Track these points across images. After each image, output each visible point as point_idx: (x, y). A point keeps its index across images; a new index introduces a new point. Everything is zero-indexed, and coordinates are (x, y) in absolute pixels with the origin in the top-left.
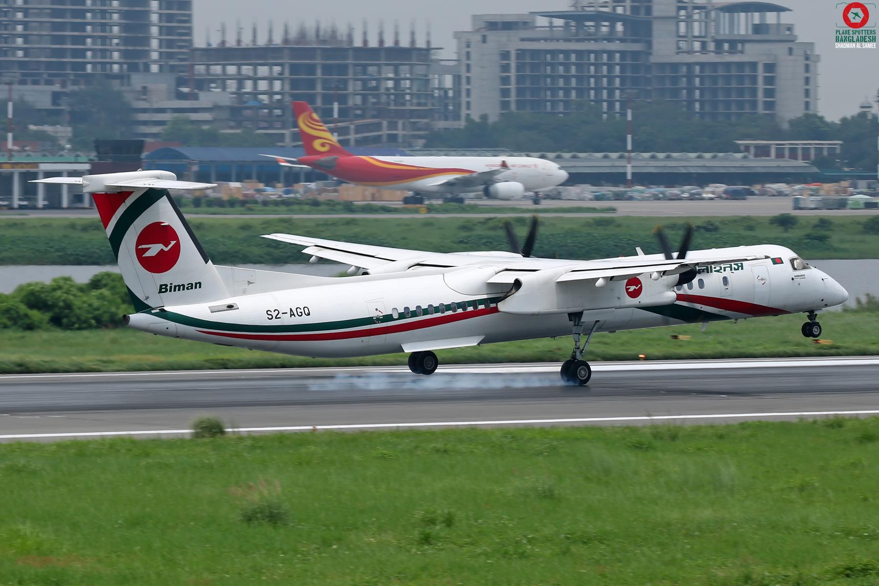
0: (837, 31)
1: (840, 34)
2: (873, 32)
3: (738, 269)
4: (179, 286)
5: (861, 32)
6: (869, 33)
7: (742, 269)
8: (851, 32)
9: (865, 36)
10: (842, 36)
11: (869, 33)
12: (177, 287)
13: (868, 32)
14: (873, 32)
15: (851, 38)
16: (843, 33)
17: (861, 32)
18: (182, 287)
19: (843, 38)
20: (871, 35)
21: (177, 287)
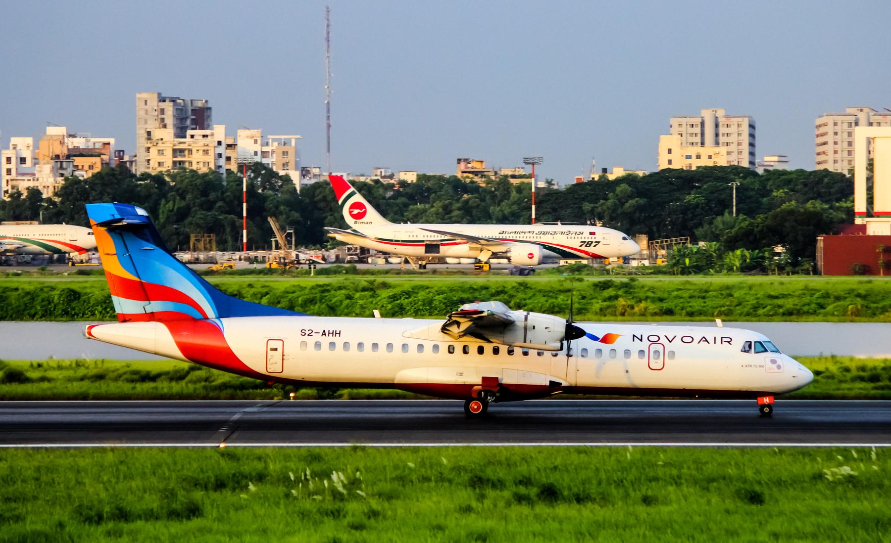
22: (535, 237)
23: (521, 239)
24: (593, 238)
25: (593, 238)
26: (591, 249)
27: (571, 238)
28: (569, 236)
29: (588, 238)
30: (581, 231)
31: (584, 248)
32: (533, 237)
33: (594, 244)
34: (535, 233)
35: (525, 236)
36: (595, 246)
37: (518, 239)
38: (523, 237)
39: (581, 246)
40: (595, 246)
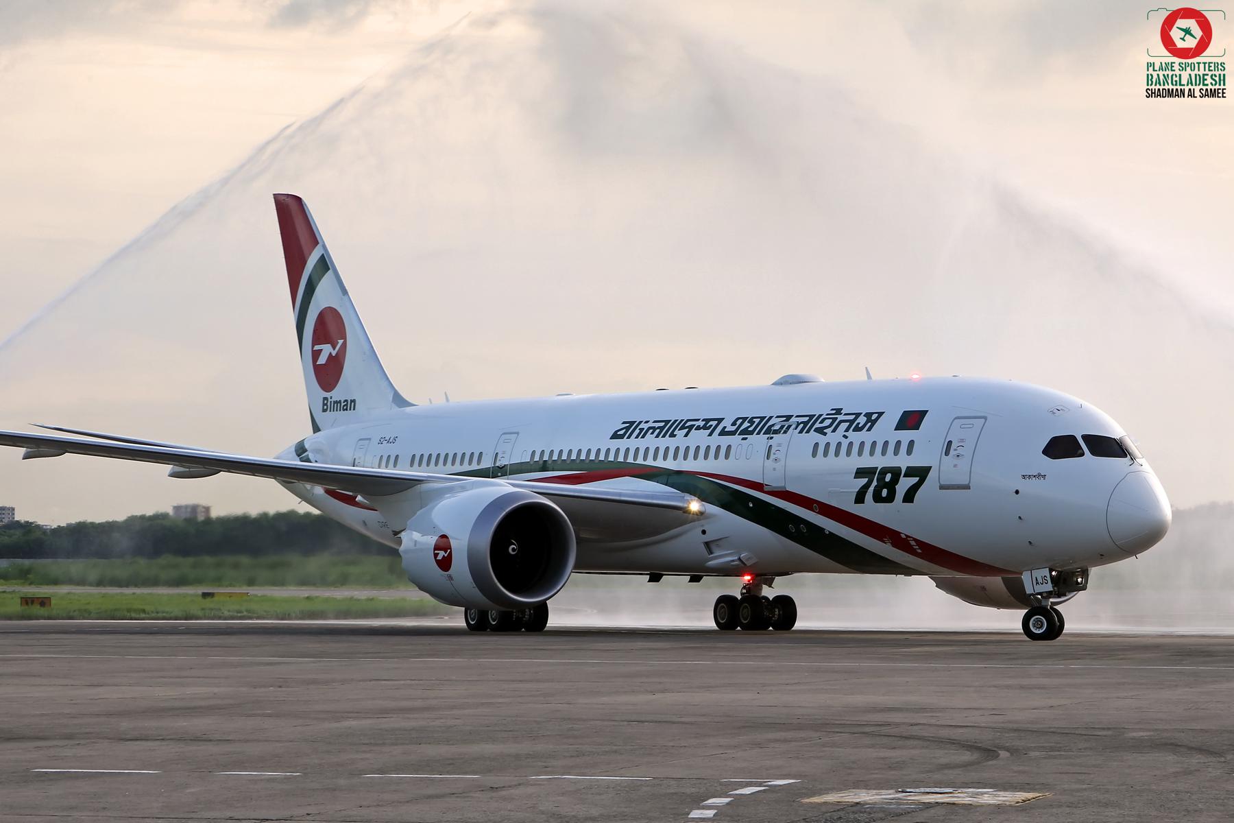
0: (1149, 65)
1: (1154, 70)
2: (1220, 67)
5: (1196, 65)
6: (1212, 68)
8: (1176, 67)
9: (1204, 75)
10: (1158, 75)
11: (1212, 68)
13: (1210, 67)
14: (1220, 67)
15: (1178, 79)
16: (1161, 68)
17: (1196, 65)
19: (1162, 77)
20: (1217, 74)
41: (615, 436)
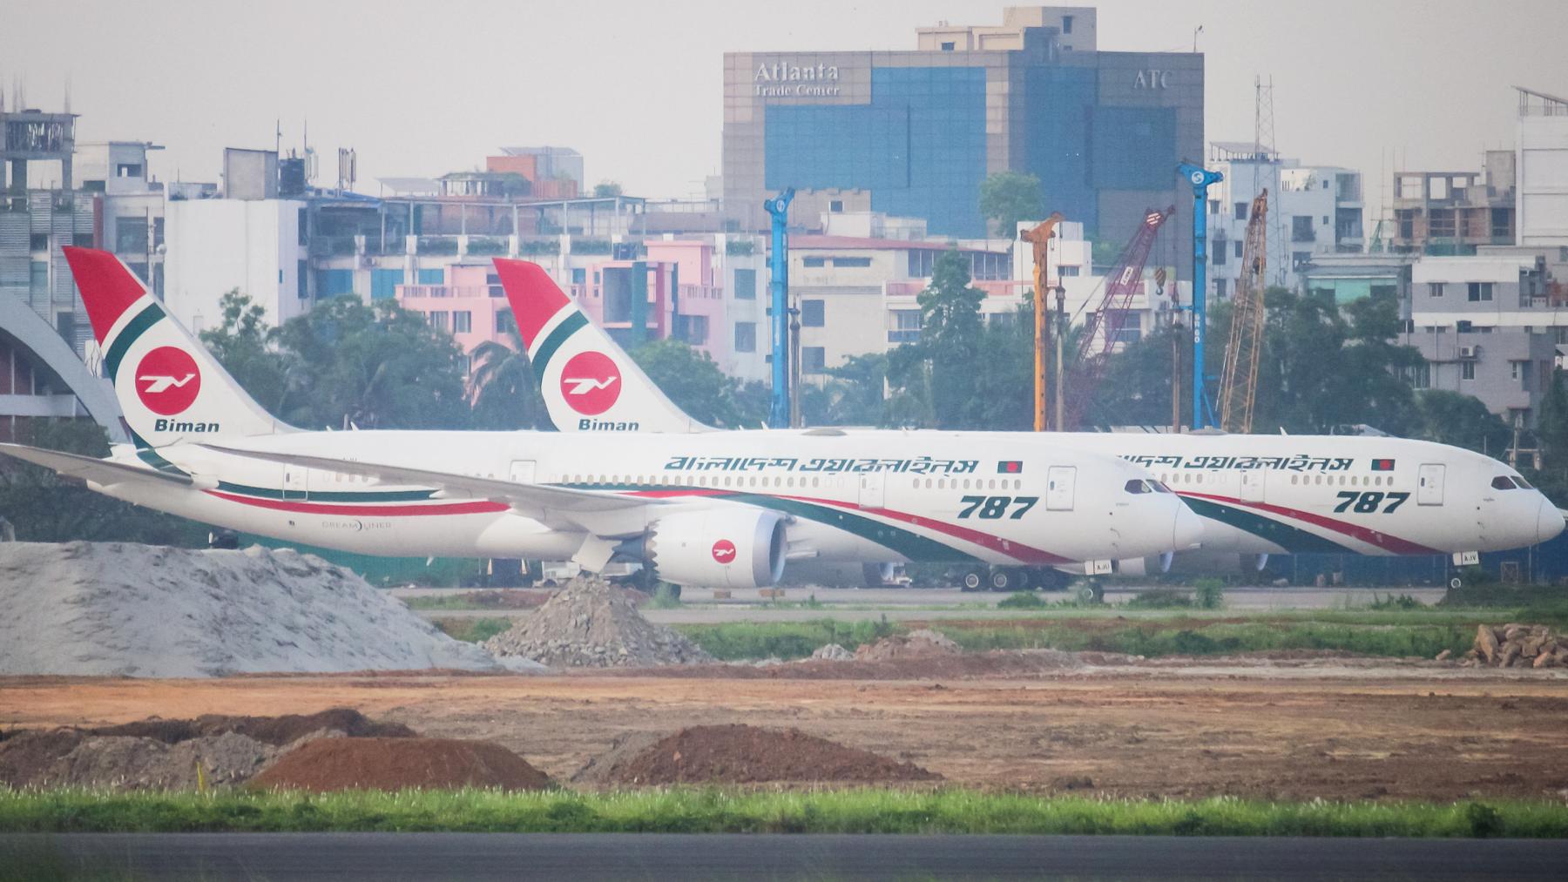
3: (962, 470)
4: (185, 425)
7: (971, 471)
12: (181, 427)
18: (188, 427)
21: (181, 427)
22: (797, 482)
23: (746, 488)
24: (1011, 485)
25: (1011, 485)
26: (1001, 527)
27: (929, 483)
28: (922, 478)
29: (992, 484)
30: (970, 459)
31: (975, 522)
32: (790, 482)
33: (1012, 508)
34: (798, 466)
35: (760, 475)
36: (1018, 515)
37: (734, 487)
38: (753, 481)
39: (965, 514)
40: (1018, 515)
41: (669, 466)
